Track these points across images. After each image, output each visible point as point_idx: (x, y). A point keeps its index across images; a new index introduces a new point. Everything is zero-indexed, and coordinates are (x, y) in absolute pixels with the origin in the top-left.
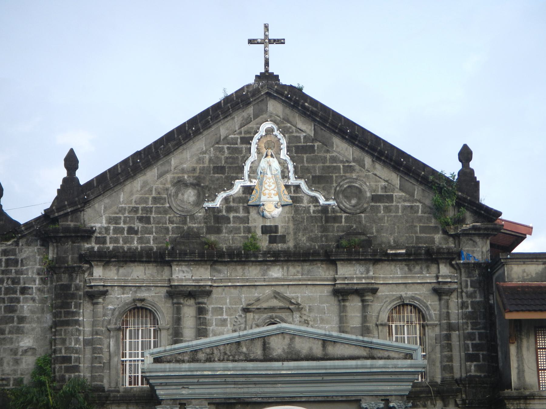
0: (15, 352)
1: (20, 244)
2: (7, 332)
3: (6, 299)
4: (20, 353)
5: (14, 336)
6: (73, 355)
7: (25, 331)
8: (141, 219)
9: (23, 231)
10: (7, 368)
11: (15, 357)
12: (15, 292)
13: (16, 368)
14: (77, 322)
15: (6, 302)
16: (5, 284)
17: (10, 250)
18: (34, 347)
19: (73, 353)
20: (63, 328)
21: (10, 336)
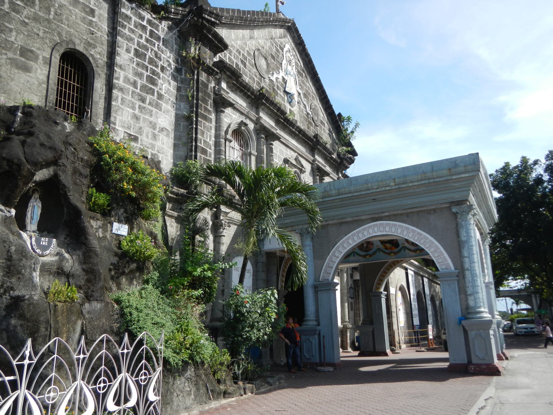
0: (154, 126)
1: (163, 24)
2: (147, 102)
3: (149, 69)
4: (158, 129)
5: (154, 110)
6: (208, 149)
7: (163, 108)
8: (242, 61)
9: (171, 12)
10: (146, 139)
11: (153, 131)
12: (157, 66)
13: (153, 142)
14: (210, 121)
15: (149, 72)
16: (149, 53)
17: (155, 23)
18: (168, 129)
19: (207, 147)
20: (203, 121)
21: (150, 107)
